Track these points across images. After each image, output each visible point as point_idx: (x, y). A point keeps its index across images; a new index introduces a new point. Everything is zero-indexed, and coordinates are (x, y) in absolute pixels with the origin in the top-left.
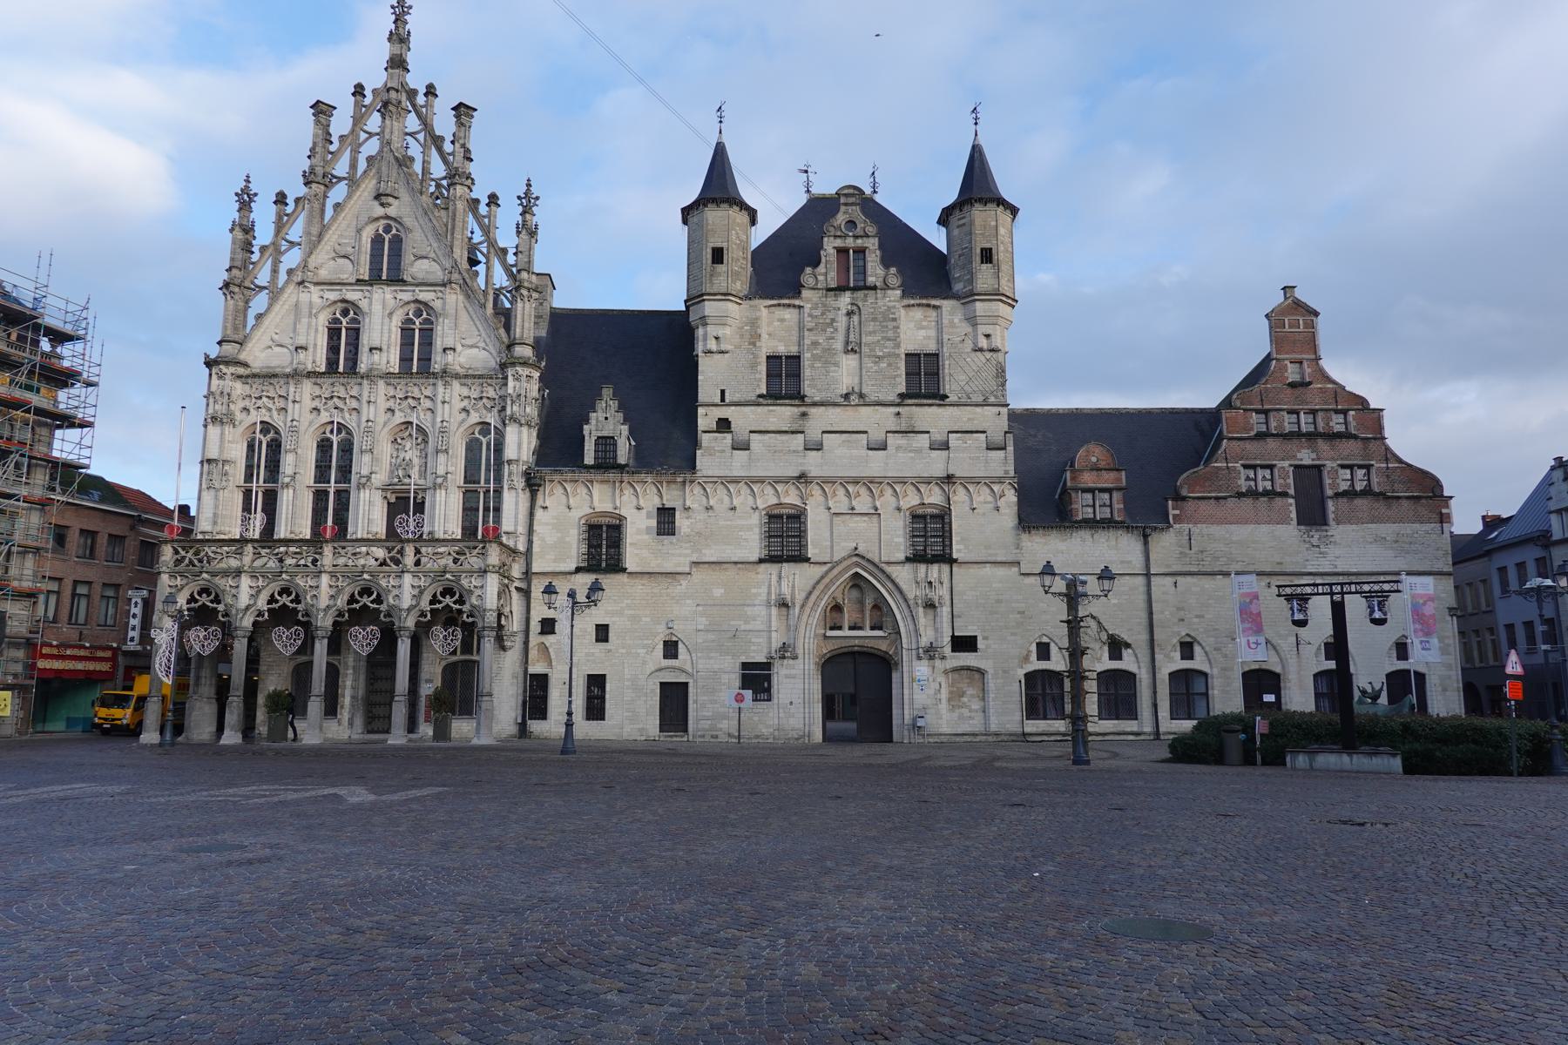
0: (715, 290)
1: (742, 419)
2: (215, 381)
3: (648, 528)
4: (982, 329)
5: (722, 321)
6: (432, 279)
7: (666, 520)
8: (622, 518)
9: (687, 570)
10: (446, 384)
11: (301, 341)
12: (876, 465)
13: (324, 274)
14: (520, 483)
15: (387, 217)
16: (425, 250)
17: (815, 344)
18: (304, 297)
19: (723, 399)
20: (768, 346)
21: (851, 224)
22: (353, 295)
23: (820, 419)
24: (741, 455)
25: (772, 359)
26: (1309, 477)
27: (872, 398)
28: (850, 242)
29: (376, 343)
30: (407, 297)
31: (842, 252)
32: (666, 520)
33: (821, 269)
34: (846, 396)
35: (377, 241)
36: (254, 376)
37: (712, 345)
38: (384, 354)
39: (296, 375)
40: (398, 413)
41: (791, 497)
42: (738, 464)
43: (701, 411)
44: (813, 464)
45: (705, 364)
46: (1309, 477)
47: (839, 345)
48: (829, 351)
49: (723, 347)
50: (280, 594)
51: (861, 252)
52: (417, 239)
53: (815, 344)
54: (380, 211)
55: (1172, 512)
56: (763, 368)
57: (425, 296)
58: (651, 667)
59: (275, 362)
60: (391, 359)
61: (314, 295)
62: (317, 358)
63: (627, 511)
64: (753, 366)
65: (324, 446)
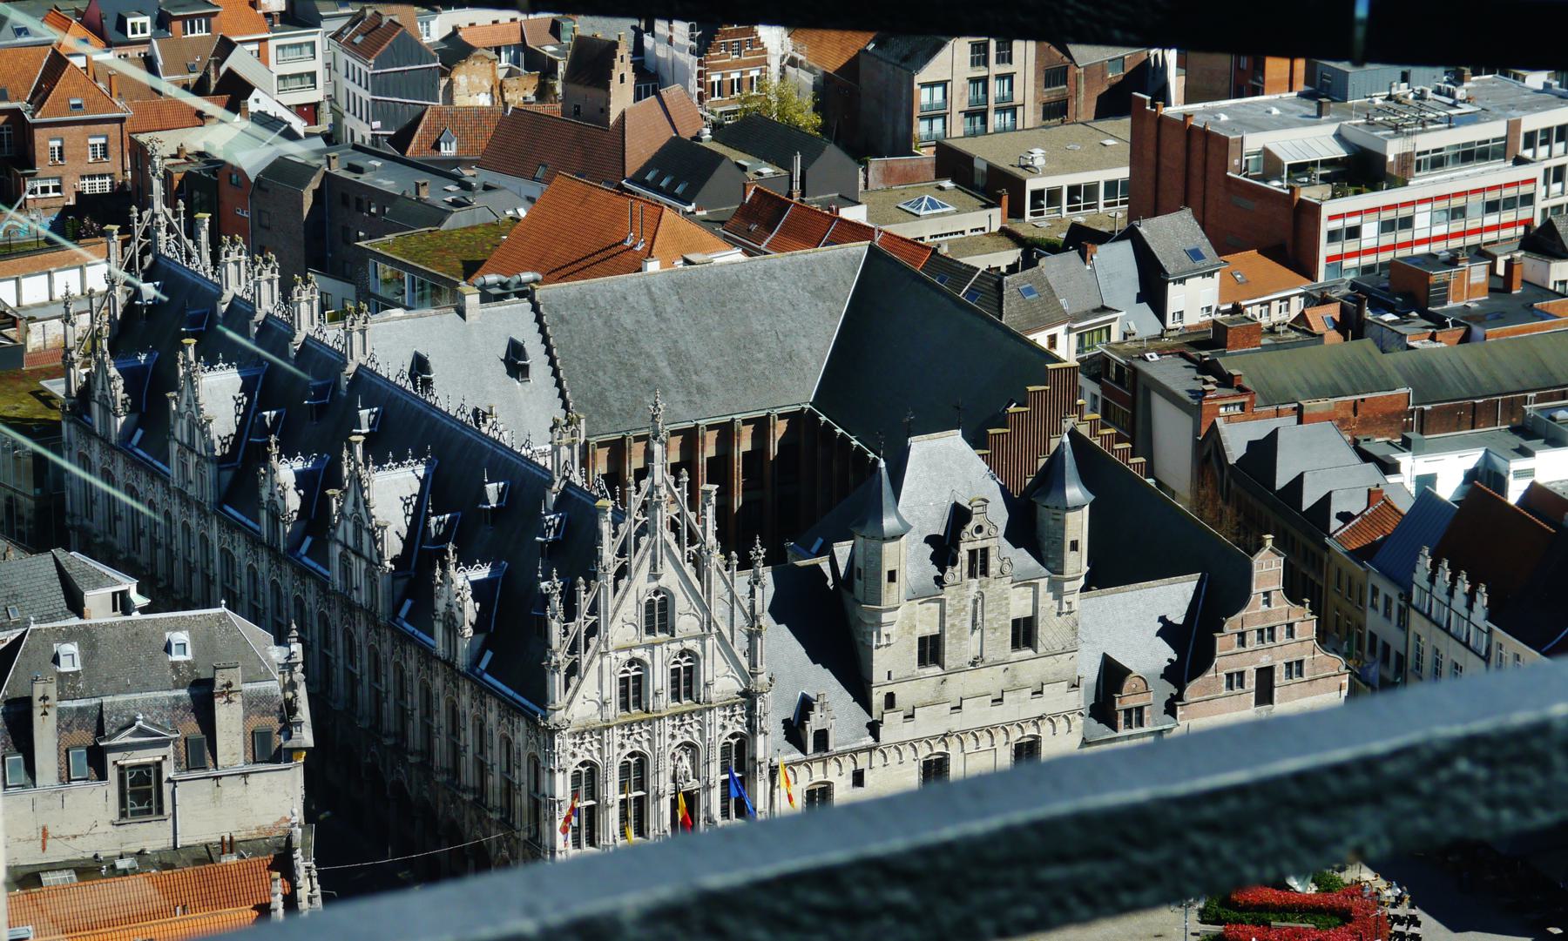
1: (904, 695)
4: (1065, 598)
5: (891, 624)
7: (858, 778)
8: (829, 783)
12: (998, 715)
14: (766, 773)
17: (953, 626)
20: (918, 633)
21: (979, 529)
22: (638, 653)
23: (957, 686)
24: (910, 725)
25: (922, 641)
26: (1265, 677)
27: (988, 661)
28: (979, 545)
29: (658, 686)
30: (676, 647)
31: (972, 553)
32: (858, 778)
33: (958, 567)
34: (973, 664)
41: (940, 748)
42: (908, 731)
44: (956, 723)
46: (1265, 677)
47: (968, 625)
48: (961, 629)
51: (985, 551)
52: (682, 603)
53: (953, 626)
55: (1179, 712)
56: (916, 650)
57: (689, 644)
63: (832, 776)
64: (910, 651)
65: (625, 769)
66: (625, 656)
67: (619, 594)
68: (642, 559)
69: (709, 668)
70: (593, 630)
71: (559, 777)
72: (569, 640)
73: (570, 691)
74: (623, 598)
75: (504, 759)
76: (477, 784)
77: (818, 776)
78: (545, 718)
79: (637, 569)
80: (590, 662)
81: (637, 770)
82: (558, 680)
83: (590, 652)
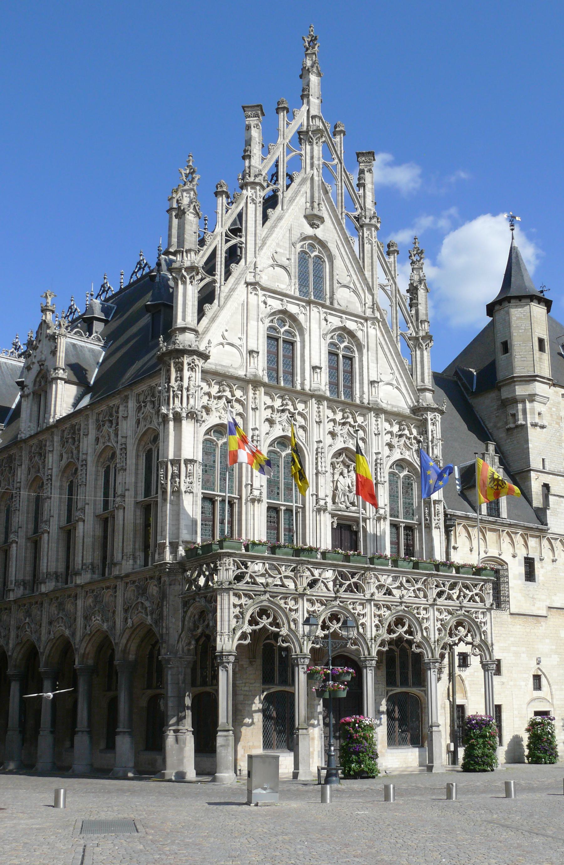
0: (542, 375)
2: (186, 374)
3: (520, 574)
6: (351, 310)
9: (543, 613)
10: (377, 416)
11: (252, 346)
13: (265, 280)
15: (315, 238)
16: (346, 280)
18: (252, 298)
19: (544, 468)
22: (293, 309)
29: (316, 363)
30: (335, 322)
35: (303, 257)
36: (215, 374)
37: (537, 420)
38: (323, 375)
39: (256, 383)
40: (340, 439)
43: (533, 474)
45: (533, 434)
49: (545, 423)
50: (331, 620)
54: (309, 231)
57: (351, 325)
58: (528, 699)
59: (226, 362)
60: (321, 382)
61: (256, 299)
62: (259, 367)
63: (506, 557)
66: (276, 305)
67: (268, 223)
68: (296, 193)
69: (372, 365)
70: (234, 255)
71: (187, 426)
72: (206, 252)
73: (205, 321)
74: (274, 227)
75: (100, 498)
76: (61, 569)
77: (493, 552)
78: (169, 338)
79: (292, 200)
80: (232, 290)
81: (288, 464)
82: (187, 296)
83: (231, 280)
